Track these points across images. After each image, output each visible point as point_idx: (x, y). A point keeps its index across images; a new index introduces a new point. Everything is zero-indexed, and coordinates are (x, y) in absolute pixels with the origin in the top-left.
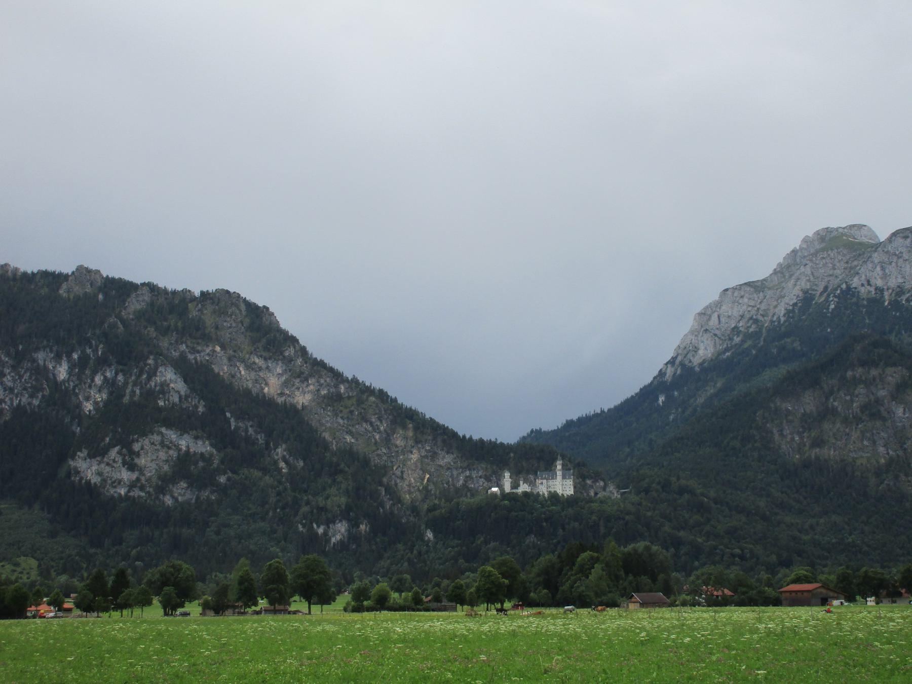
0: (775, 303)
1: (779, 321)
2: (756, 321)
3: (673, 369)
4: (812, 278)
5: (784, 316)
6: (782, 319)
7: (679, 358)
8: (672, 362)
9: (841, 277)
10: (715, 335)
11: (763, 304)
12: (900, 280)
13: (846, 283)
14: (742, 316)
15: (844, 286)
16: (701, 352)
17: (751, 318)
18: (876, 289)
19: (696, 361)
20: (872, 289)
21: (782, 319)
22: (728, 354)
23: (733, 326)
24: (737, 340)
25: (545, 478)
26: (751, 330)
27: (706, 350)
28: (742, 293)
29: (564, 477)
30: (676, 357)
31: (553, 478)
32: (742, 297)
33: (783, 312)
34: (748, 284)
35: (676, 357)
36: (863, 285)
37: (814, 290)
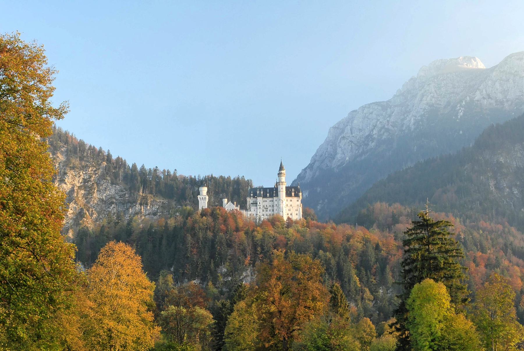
0: (402, 117)
2: (387, 130)
4: (436, 95)
5: (414, 124)
6: (413, 127)
7: (317, 164)
8: (311, 166)
10: (352, 142)
13: (469, 96)
14: (375, 126)
15: (468, 98)
16: (339, 156)
17: (383, 127)
18: (496, 101)
19: (334, 164)
20: (493, 101)
21: (413, 127)
22: (363, 157)
23: (367, 134)
24: (372, 145)
25: (260, 196)
26: (384, 137)
27: (344, 154)
28: (371, 110)
29: (289, 194)
30: (314, 163)
31: (271, 196)
32: (371, 113)
33: (412, 121)
34: (376, 104)
35: (314, 163)
36: (484, 98)
37: (438, 104)
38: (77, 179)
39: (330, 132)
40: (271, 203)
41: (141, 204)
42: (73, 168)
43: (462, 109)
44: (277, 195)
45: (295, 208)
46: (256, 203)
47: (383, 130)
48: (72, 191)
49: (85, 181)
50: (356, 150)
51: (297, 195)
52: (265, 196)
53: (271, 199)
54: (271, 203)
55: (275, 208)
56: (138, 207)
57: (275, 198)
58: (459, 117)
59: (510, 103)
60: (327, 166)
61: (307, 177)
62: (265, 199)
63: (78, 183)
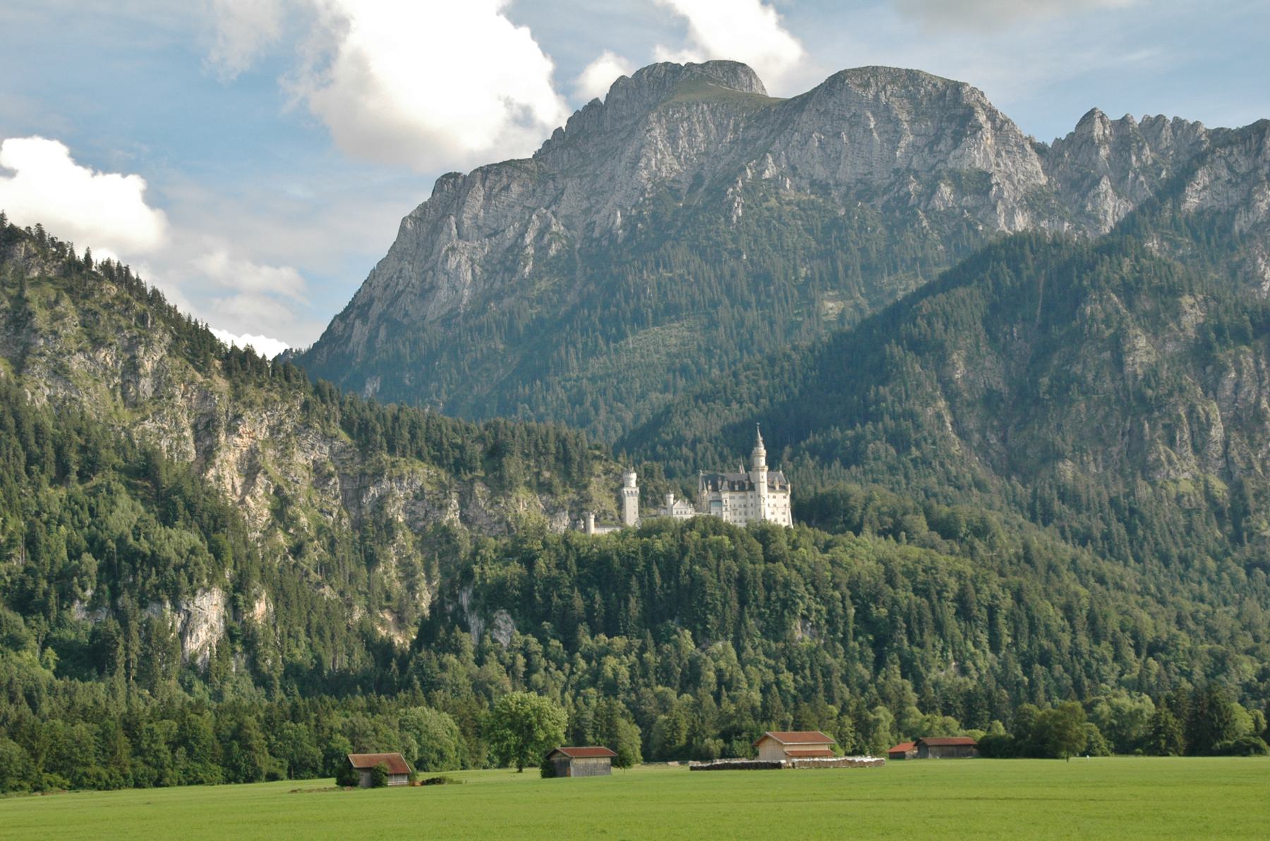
0: (585, 204)
1: (612, 239)
3: (366, 330)
5: (623, 226)
9: (727, 159)
11: (563, 204)
12: (861, 169)
18: (813, 183)
23: (507, 244)
29: (771, 488)
31: (742, 489)
38: (258, 426)
39: (403, 228)
40: (742, 502)
41: (390, 479)
42: (250, 405)
43: (738, 199)
44: (752, 487)
45: (782, 510)
46: (720, 501)
47: (547, 237)
48: (253, 452)
49: (274, 430)
50: (485, 281)
51: (783, 488)
52: (732, 489)
53: (742, 494)
54: (742, 502)
55: (750, 509)
56: (386, 485)
57: (749, 494)
58: (735, 219)
59: (843, 189)
60: (406, 314)
61: (354, 340)
62: (733, 494)
63: (263, 434)
